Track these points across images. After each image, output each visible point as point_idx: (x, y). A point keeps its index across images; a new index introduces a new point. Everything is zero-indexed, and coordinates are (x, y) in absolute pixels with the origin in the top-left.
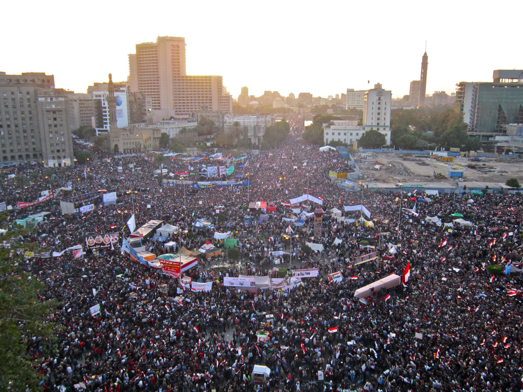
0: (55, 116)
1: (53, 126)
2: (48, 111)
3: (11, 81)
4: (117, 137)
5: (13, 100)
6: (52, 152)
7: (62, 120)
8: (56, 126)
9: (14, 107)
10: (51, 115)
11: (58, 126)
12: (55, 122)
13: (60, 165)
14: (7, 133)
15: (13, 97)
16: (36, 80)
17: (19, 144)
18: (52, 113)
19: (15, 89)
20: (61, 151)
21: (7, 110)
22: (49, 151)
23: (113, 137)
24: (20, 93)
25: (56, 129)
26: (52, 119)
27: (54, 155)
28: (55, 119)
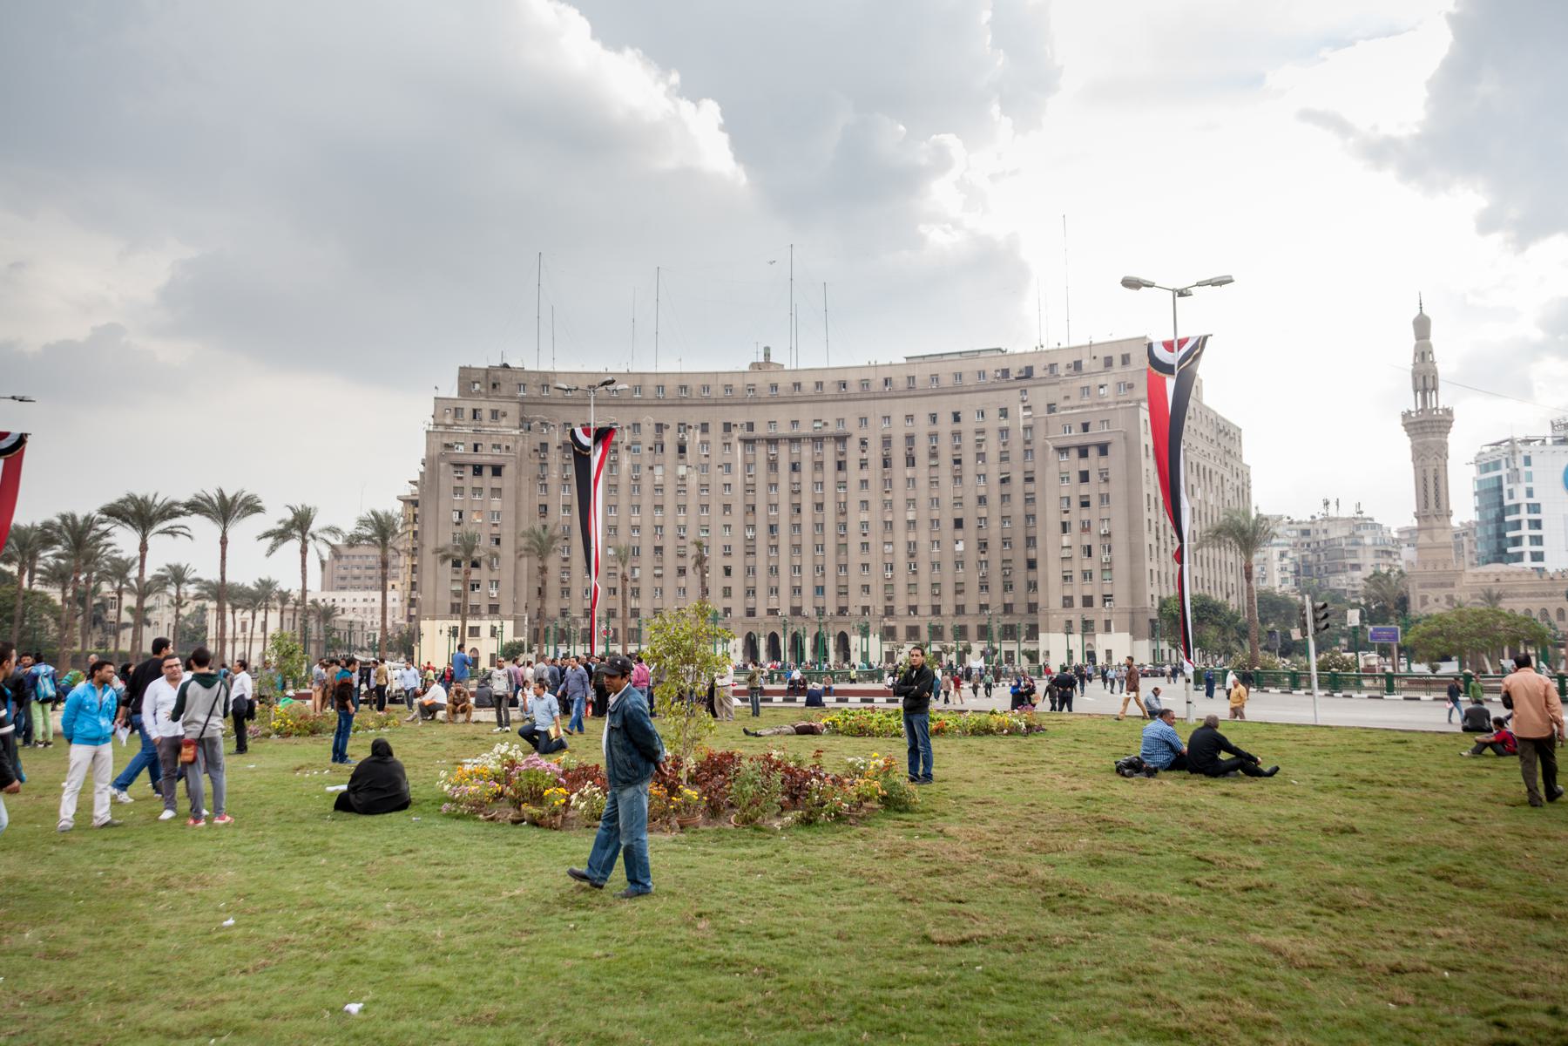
0: (1084, 465)
1: (1075, 503)
2: (1062, 450)
3: (1006, 372)
4: (1442, 585)
5: (1004, 432)
6: (1068, 602)
7: (1106, 481)
8: (1085, 504)
9: (1002, 459)
10: (1073, 463)
11: (1094, 501)
12: (1084, 489)
13: (1091, 656)
14: (974, 545)
15: (1005, 423)
16: (1085, 362)
17: (1008, 587)
18: (1074, 453)
19: (1011, 399)
20: (1097, 601)
21: (982, 470)
22: (1055, 602)
23: (1423, 586)
24: (1027, 408)
25: (1085, 514)
26: (1075, 477)
27: (1072, 617)
28: (1084, 477)
